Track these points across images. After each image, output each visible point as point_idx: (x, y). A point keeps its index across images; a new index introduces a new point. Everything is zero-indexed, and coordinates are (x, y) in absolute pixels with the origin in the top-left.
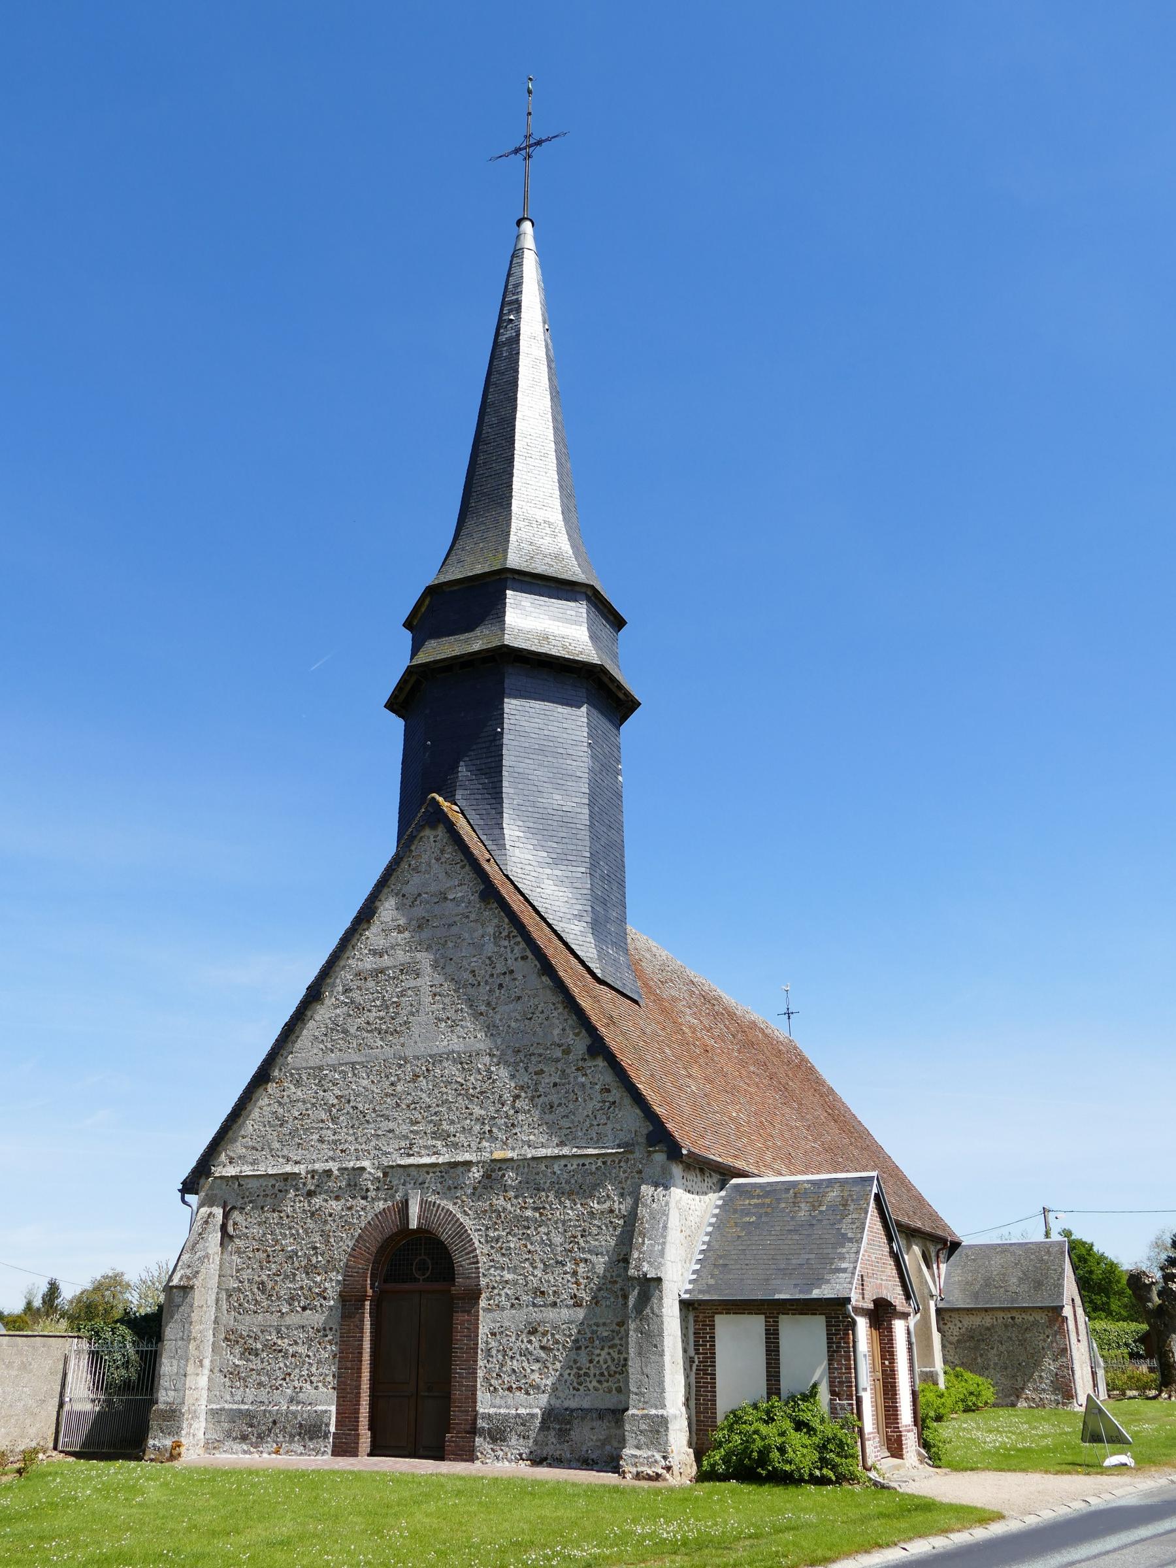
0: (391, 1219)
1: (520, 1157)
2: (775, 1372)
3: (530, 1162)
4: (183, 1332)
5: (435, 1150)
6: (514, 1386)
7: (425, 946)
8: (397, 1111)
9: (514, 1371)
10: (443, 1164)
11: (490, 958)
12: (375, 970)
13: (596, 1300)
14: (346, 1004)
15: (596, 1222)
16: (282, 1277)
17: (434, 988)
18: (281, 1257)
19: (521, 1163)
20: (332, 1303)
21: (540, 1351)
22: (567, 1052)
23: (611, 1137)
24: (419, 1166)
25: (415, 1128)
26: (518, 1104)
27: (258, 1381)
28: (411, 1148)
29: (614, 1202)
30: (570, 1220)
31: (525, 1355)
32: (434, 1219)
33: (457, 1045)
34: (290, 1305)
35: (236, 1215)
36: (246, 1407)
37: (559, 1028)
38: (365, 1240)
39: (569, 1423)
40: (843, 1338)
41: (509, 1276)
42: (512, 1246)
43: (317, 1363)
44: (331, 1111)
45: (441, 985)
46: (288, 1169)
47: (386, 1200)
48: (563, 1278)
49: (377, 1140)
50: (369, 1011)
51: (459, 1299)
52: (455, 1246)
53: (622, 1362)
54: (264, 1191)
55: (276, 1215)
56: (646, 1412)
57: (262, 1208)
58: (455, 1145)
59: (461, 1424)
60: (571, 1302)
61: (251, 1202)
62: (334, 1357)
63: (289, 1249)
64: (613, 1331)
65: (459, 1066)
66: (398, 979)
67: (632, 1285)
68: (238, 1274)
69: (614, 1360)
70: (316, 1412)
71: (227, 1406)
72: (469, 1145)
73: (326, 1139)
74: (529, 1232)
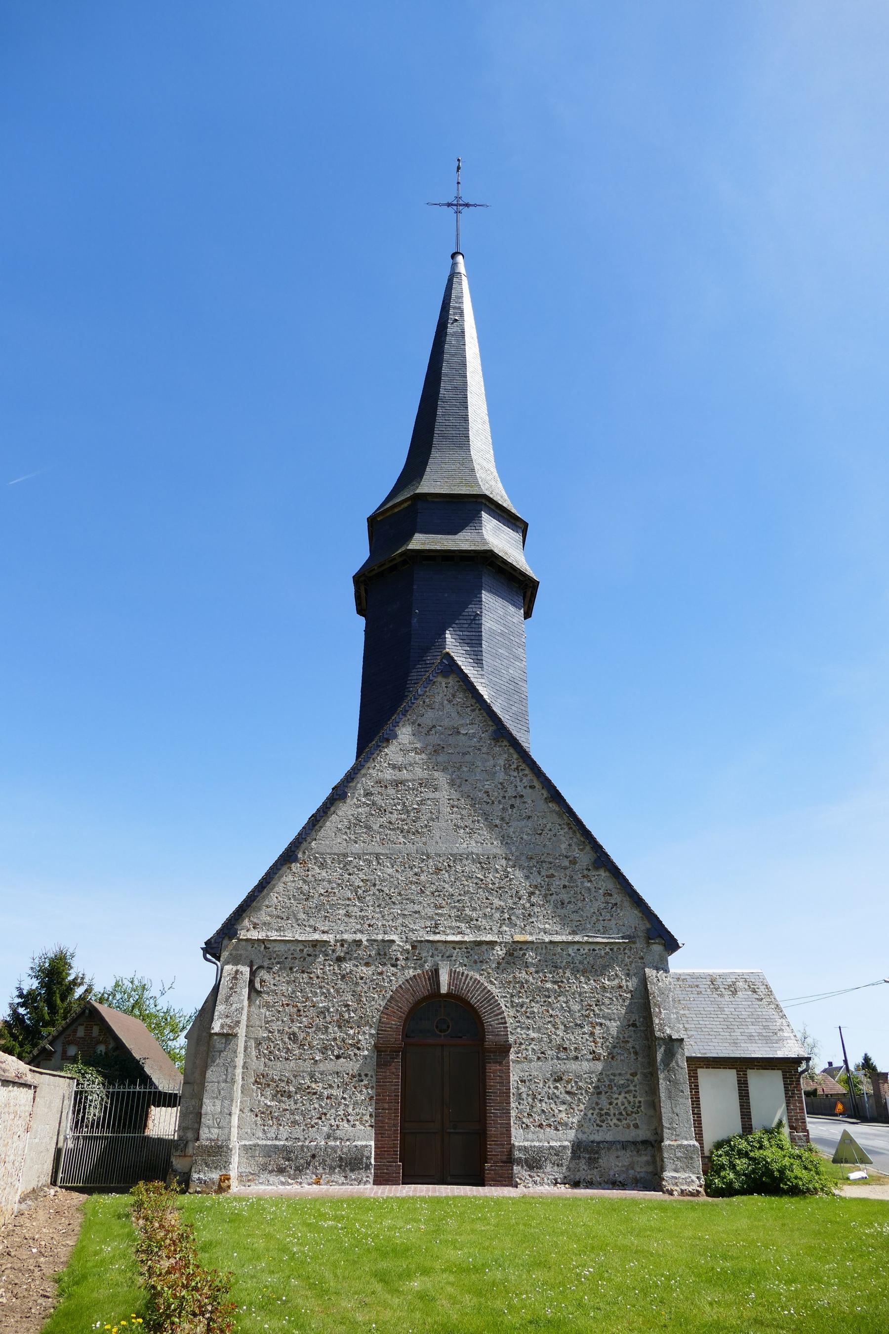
0: (422, 984)
1: (538, 941)
2: (747, 1112)
3: (547, 945)
4: (226, 1075)
5: (459, 930)
6: (544, 1124)
7: (442, 767)
8: (422, 897)
9: (543, 1111)
10: (470, 942)
11: (501, 784)
12: (395, 781)
13: (612, 1056)
14: (368, 805)
15: (608, 995)
16: (313, 1029)
17: (451, 801)
18: (312, 1012)
19: (539, 945)
20: (366, 1053)
21: (566, 1095)
22: (573, 862)
23: (616, 931)
24: (446, 942)
25: (440, 911)
26: (534, 899)
27: (292, 1120)
28: (436, 928)
29: (622, 980)
30: (586, 992)
31: (552, 1099)
32: (463, 986)
33: (473, 846)
34: (323, 1054)
35: (263, 974)
36: (282, 1143)
37: (565, 842)
38: (397, 1001)
39: (597, 1153)
40: (796, 1087)
41: (533, 1035)
42: (536, 1010)
43: (354, 1104)
44: (357, 891)
45: (459, 800)
46: (316, 936)
47: (415, 969)
48: (582, 1038)
49: (403, 918)
50: (391, 813)
51: (491, 1052)
52: (484, 1009)
53: (637, 1104)
54: (292, 954)
55: (305, 975)
56: (679, 1143)
57: (291, 969)
58: (478, 928)
59: (498, 1155)
60: (591, 1057)
61: (278, 963)
62: (371, 1098)
63: (321, 1005)
64: (628, 1080)
65: (478, 865)
66: (418, 790)
67: (659, 1044)
68: (267, 1025)
69: (629, 1103)
70: (356, 1147)
71: (260, 1142)
72: (491, 929)
73: (353, 914)
74: (550, 1000)
